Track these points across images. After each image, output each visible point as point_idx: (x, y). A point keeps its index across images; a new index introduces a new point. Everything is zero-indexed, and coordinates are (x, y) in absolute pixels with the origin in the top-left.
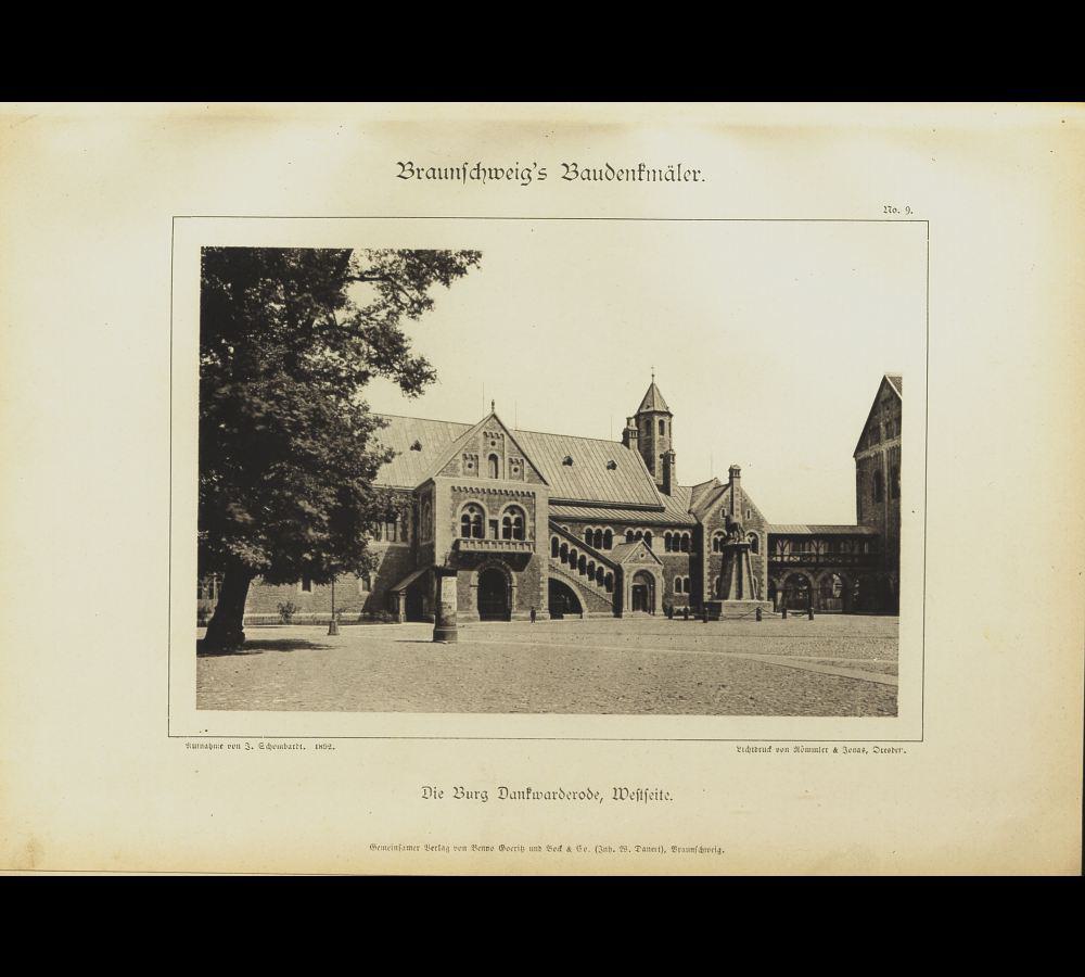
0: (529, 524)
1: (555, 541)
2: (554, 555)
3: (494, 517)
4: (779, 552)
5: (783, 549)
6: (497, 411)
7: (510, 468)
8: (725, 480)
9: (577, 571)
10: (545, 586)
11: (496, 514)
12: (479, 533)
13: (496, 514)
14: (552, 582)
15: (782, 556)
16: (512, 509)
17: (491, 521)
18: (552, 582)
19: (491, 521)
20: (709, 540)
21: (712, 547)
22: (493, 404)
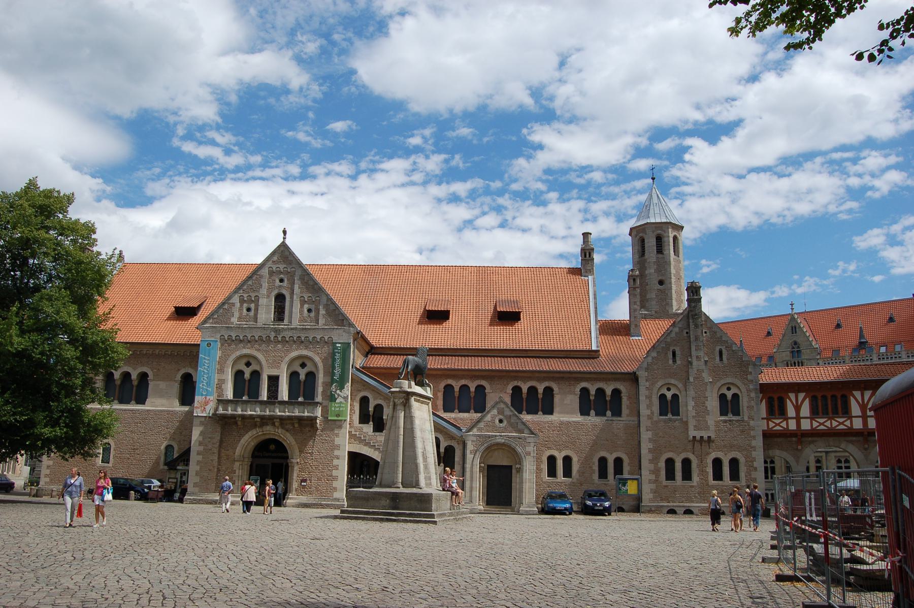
1: (364, 401)
2: (364, 419)
3: (274, 372)
4: (791, 412)
5: (798, 408)
6: (288, 242)
11: (278, 367)
12: (254, 393)
13: (278, 367)
14: (353, 456)
15: (798, 418)
18: (353, 456)
20: (649, 397)
22: (285, 232)
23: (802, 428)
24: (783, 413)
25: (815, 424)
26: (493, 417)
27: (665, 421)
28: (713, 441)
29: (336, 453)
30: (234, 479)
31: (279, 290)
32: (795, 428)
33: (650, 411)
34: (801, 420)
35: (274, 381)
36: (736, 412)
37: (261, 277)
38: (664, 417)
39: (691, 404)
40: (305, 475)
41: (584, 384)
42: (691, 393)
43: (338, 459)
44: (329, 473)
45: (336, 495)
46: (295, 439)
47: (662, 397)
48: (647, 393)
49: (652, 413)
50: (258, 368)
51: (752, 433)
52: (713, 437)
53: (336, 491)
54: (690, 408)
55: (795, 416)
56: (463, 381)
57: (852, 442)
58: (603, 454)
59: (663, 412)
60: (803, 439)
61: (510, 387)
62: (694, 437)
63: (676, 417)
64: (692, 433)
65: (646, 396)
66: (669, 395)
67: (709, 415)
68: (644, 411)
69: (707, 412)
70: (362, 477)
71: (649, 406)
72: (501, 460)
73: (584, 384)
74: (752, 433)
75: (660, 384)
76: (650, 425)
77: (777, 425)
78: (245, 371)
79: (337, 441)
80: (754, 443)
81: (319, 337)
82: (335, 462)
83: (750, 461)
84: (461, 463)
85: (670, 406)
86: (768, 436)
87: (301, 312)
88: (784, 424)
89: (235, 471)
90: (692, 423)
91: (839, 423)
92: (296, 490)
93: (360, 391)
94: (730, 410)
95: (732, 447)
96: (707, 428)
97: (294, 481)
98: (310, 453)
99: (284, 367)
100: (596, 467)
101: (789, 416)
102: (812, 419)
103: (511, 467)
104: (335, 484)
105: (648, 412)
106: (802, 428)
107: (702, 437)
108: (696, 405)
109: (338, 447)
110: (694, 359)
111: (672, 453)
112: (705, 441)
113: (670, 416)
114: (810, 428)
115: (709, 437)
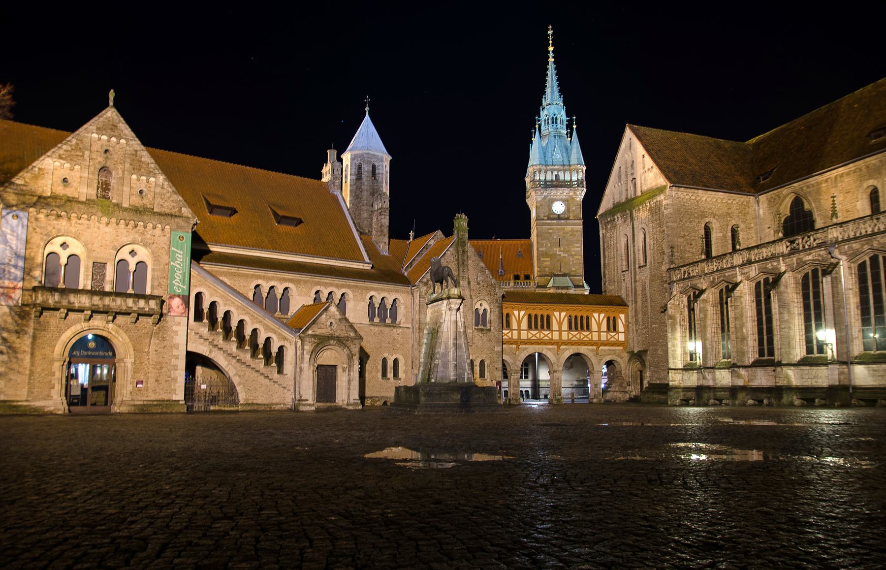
4: (514, 325)
5: (519, 323)
15: (519, 330)
26: (327, 320)
30: (52, 382)
40: (141, 377)
41: (372, 293)
43: (177, 358)
45: (175, 398)
46: (129, 336)
56: (273, 282)
57: (549, 349)
58: (386, 355)
60: (521, 346)
61: (314, 291)
73: (372, 293)
84: (293, 362)
89: (54, 373)
91: (545, 334)
92: (131, 393)
97: (129, 383)
98: (146, 352)
100: (380, 368)
103: (335, 366)
109: (176, 346)
110: (461, 278)
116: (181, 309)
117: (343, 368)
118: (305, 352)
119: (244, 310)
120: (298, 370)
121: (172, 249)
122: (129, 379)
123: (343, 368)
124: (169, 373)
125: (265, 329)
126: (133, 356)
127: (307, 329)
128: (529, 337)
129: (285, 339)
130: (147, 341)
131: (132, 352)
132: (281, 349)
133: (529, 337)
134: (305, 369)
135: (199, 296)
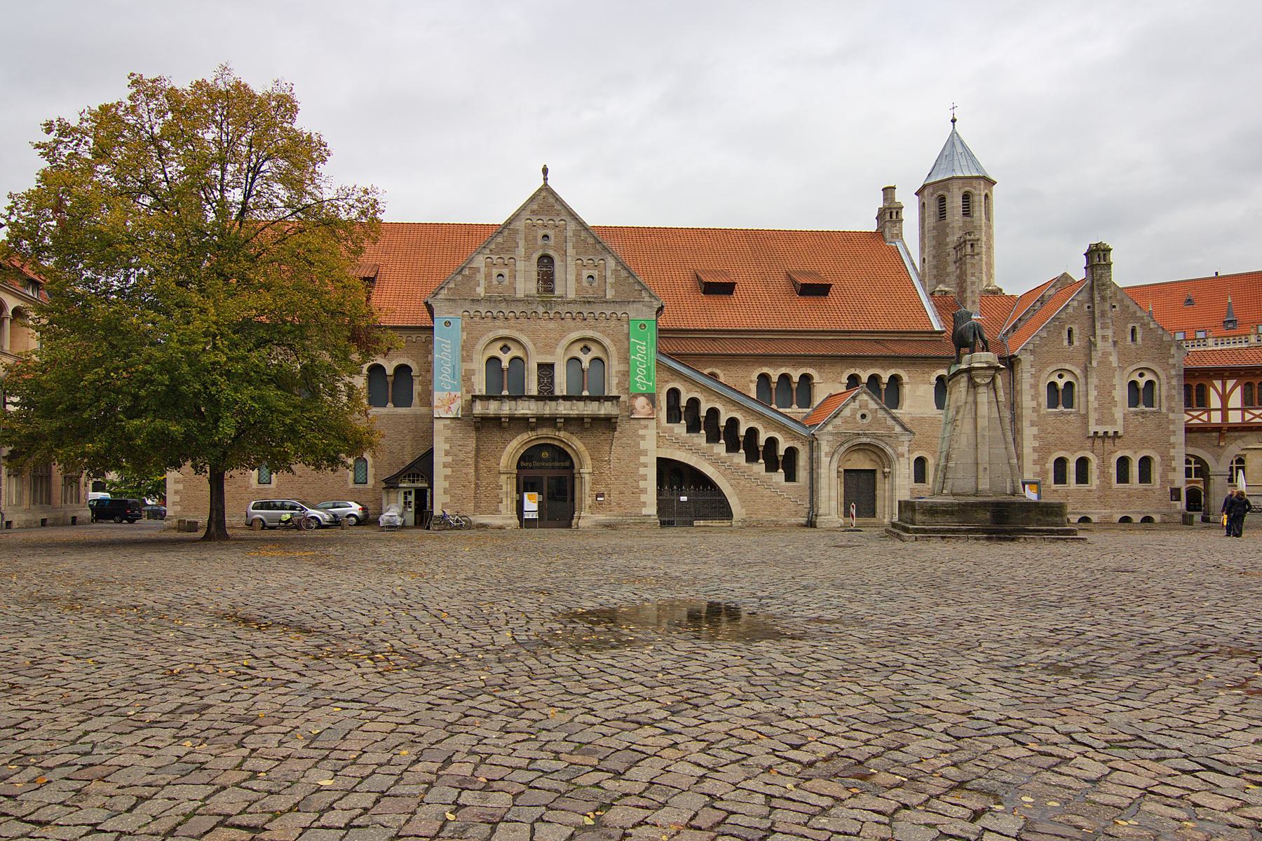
0: (614, 366)
1: (674, 394)
2: (674, 415)
3: (547, 359)
4: (1215, 401)
5: (1224, 398)
7: (579, 275)
8: (1078, 272)
9: (720, 448)
10: (652, 473)
11: (552, 353)
13: (552, 353)
14: (661, 462)
15: (1224, 410)
16: (586, 343)
17: (540, 366)
18: (661, 462)
19: (540, 366)
20: (1035, 386)
21: (1044, 399)
23: (1230, 421)
24: (1203, 402)
25: (1248, 416)
27: (1055, 414)
28: (1120, 437)
29: (643, 459)
31: (544, 251)
32: (1220, 422)
33: (1035, 402)
34: (1229, 412)
35: (546, 370)
36: (1150, 403)
37: (516, 231)
38: (1054, 410)
39: (1093, 394)
40: (602, 489)
42: (1094, 380)
44: (635, 484)
46: (584, 444)
47: (1052, 385)
48: (1032, 381)
49: (1039, 405)
50: (520, 353)
51: (1171, 427)
52: (1121, 433)
53: (645, 507)
54: (1091, 398)
55: (1220, 407)
59: (1052, 403)
62: (1096, 433)
63: (1070, 410)
64: (1093, 428)
65: (1031, 385)
66: (1061, 383)
67: (1116, 406)
68: (1027, 401)
69: (1113, 403)
70: (675, 487)
71: (1035, 397)
72: (862, 462)
74: (1171, 427)
75: (1050, 369)
76: (1035, 419)
77: (1197, 417)
78: (502, 358)
79: (643, 445)
80: (1173, 439)
81: (608, 313)
82: (642, 471)
83: (1167, 460)
84: (808, 467)
85: (1061, 396)
86: (1189, 430)
87: (578, 279)
88: (1204, 417)
90: (1093, 417)
92: (590, 507)
93: (667, 382)
94: (1141, 401)
95: (1143, 443)
96: (1113, 422)
99: (560, 350)
101: (1212, 407)
102: (1243, 410)
103: (874, 472)
104: (643, 498)
105: (1034, 404)
106: (1230, 421)
107: (1106, 433)
108: (1100, 394)
109: (645, 453)
111: (1064, 452)
112: (1109, 437)
113: (1061, 408)
114: (1240, 421)
115: (1116, 433)
116: (647, 409)
117: (884, 473)
118: (823, 454)
119: (735, 406)
120: (815, 477)
121: (632, 340)
122: (587, 491)
123: (884, 473)
124: (635, 484)
125: (765, 428)
126: (590, 466)
127: (826, 424)
128: (1246, 419)
129: (795, 436)
130: (607, 448)
131: (590, 462)
132: (792, 452)
133: (1246, 419)
134: (823, 476)
135: (674, 394)
